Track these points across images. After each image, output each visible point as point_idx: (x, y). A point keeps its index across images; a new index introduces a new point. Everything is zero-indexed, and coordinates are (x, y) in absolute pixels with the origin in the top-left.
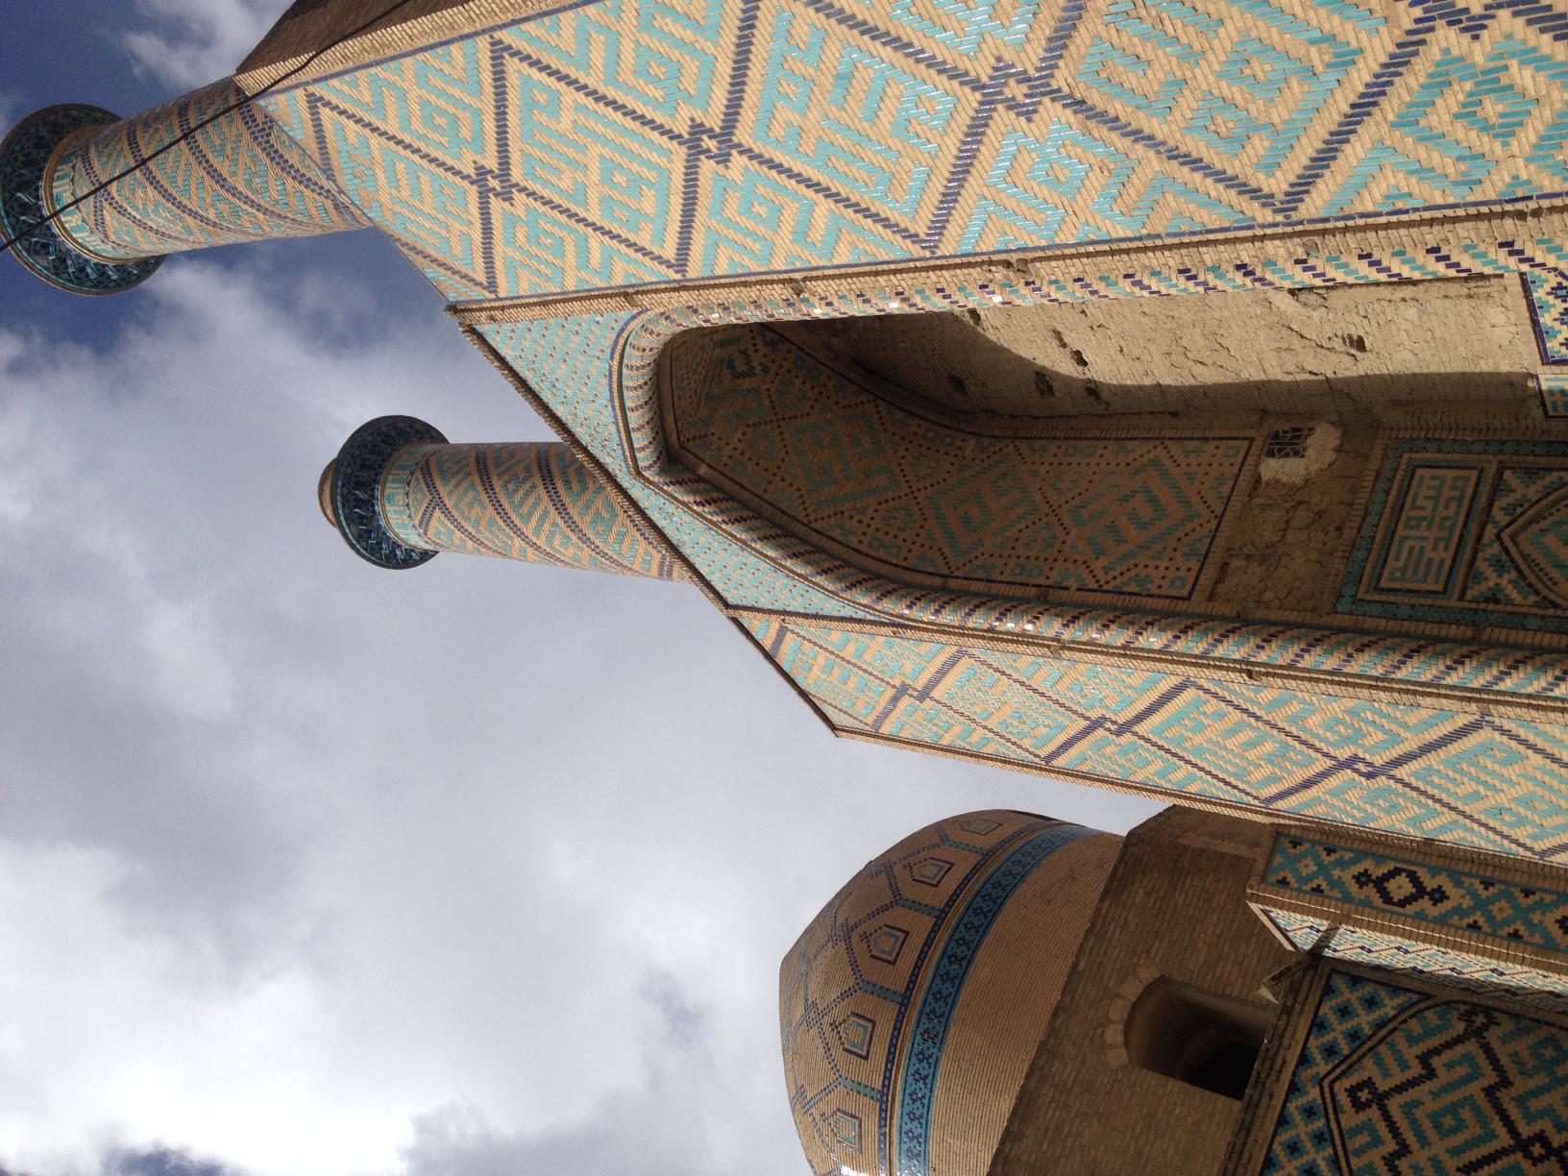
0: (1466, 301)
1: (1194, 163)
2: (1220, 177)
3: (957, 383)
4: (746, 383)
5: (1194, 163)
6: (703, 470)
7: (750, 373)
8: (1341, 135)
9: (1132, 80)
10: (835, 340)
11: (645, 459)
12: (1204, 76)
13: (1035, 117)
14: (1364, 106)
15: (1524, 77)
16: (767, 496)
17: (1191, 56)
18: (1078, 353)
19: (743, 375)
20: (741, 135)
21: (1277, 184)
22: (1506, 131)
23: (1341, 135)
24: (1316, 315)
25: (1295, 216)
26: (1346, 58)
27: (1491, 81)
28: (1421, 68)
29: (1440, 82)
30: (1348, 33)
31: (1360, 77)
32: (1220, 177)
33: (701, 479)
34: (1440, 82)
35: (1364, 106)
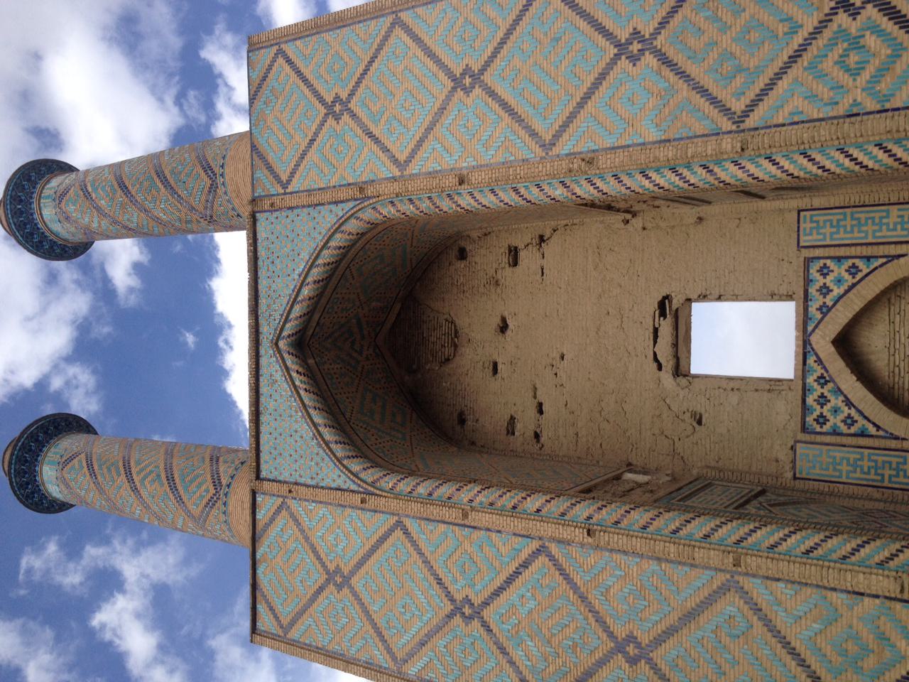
0: (765, 393)
1: (703, 91)
2: (714, 101)
3: (462, 421)
4: (355, 355)
5: (703, 91)
6: (311, 361)
7: (360, 353)
8: (779, 76)
9: (692, 42)
10: (407, 378)
11: (289, 329)
12: (725, 40)
13: (638, 63)
14: (794, 58)
15: (871, 41)
16: (335, 397)
17: (725, 28)
18: (540, 405)
19: (356, 351)
20: (487, 77)
21: (738, 106)
22: (855, 73)
23: (779, 76)
24: (682, 393)
25: (742, 126)
26: (793, 31)
27: (856, 44)
28: (827, 33)
29: (832, 43)
30: (799, 16)
31: (798, 40)
32: (714, 101)
33: (307, 364)
34: (832, 43)
35: (794, 58)
